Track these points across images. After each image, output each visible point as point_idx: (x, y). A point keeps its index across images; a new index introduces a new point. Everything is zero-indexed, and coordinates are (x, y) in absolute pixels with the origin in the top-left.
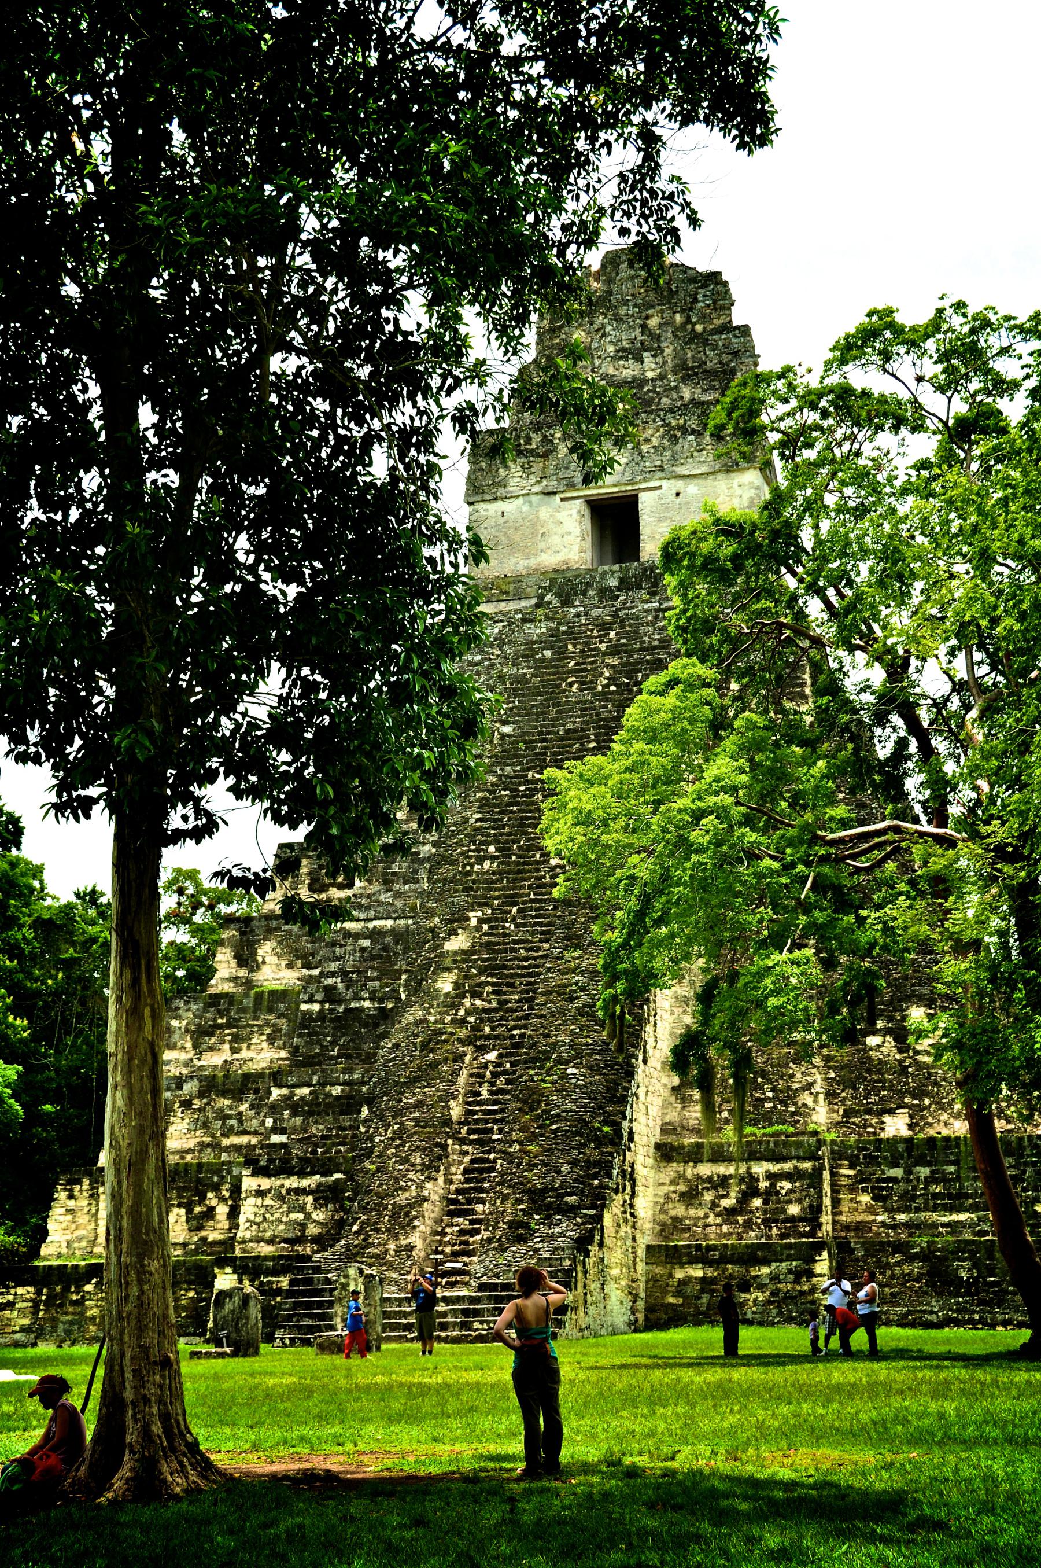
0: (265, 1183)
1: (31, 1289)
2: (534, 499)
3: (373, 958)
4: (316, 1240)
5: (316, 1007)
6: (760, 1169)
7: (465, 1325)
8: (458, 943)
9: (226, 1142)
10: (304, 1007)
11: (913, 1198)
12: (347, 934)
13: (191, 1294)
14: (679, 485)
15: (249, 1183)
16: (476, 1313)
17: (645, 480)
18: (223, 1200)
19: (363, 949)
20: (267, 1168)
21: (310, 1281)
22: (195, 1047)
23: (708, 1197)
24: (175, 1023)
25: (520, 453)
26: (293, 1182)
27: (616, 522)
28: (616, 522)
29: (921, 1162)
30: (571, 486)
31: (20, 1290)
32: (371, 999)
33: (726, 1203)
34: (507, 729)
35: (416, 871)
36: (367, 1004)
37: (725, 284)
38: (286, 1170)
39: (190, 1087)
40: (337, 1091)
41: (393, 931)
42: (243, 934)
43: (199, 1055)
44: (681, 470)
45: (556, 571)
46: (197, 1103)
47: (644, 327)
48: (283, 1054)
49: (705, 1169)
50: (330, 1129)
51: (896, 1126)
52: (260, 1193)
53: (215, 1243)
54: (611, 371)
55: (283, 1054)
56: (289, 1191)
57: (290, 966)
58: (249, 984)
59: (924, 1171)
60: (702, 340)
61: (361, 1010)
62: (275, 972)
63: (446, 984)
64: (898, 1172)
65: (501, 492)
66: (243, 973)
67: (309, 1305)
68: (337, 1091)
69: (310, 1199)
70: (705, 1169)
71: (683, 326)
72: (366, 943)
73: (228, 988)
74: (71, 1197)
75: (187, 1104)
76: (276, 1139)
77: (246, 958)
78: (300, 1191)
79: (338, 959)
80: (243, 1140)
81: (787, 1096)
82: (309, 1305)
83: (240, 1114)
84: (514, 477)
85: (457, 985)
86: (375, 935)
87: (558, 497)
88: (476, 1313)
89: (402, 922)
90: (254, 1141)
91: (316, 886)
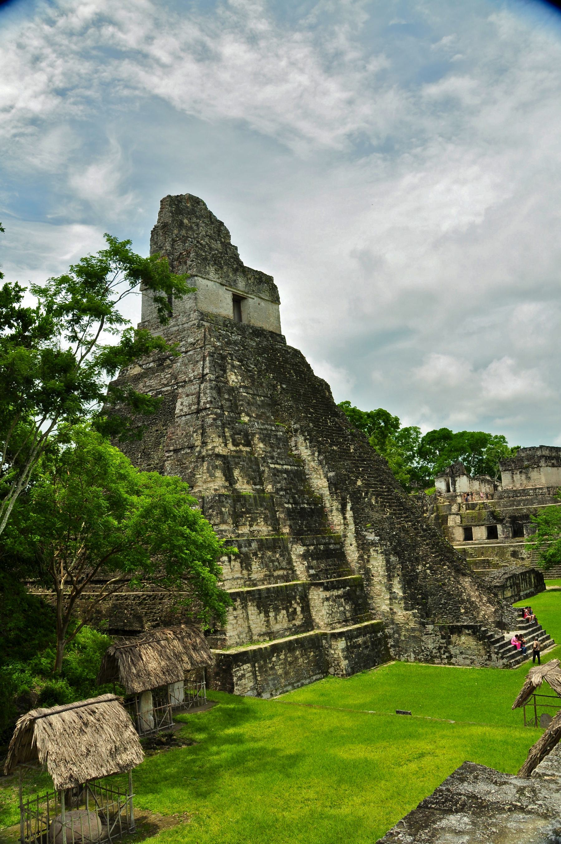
0: (328, 594)
1: (249, 665)
2: (217, 284)
5: (290, 506)
9: (276, 573)
10: (286, 505)
13: (312, 654)
14: (259, 300)
17: (251, 294)
19: (285, 479)
20: (327, 586)
26: (335, 593)
30: (230, 286)
31: (245, 667)
32: (307, 504)
35: (279, 444)
36: (306, 506)
39: (254, 545)
41: (292, 470)
42: (224, 463)
50: (326, 566)
56: (336, 596)
57: (248, 483)
61: (304, 508)
66: (227, 484)
69: (343, 600)
72: (285, 476)
74: (235, 609)
75: (255, 554)
78: (339, 597)
79: (279, 482)
80: (281, 573)
83: (277, 559)
86: (286, 471)
87: (225, 287)
89: (293, 467)
91: (235, 444)
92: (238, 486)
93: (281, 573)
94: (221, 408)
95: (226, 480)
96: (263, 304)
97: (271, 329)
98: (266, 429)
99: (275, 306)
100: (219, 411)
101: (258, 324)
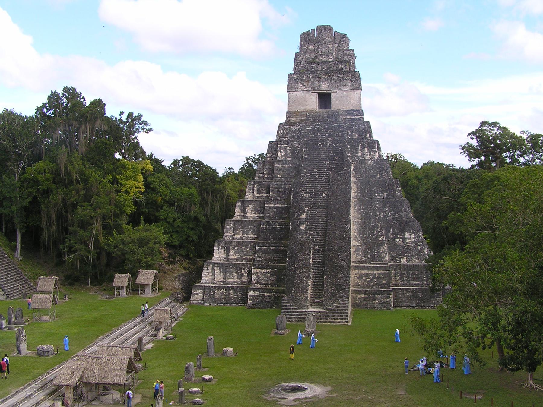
0: (258, 270)
3: (277, 214)
4: (271, 284)
5: (265, 226)
6: (376, 272)
7: (326, 319)
8: (304, 216)
9: (244, 257)
10: (262, 226)
11: (408, 278)
12: (270, 207)
14: (342, 91)
15: (254, 270)
16: (328, 316)
18: (246, 272)
19: (274, 212)
21: (286, 306)
22: (233, 232)
23: (364, 278)
24: (227, 227)
25: (301, 80)
27: (325, 99)
28: (325, 99)
29: (410, 270)
30: (314, 90)
33: (368, 280)
34: (306, 156)
37: (348, 38)
38: (263, 267)
39: (234, 244)
40: (273, 248)
41: (281, 207)
43: (234, 235)
44: (342, 88)
45: (310, 111)
46: (236, 248)
47: (328, 47)
48: (255, 236)
49: (363, 272)
51: (404, 261)
52: (257, 273)
53: (244, 282)
54: (321, 58)
55: (255, 236)
57: (255, 213)
58: (245, 217)
59: (411, 272)
60: (343, 51)
61: (276, 227)
62: (251, 214)
63: (302, 227)
64: (405, 272)
65: (297, 90)
66: (242, 214)
67: (287, 312)
68: (273, 248)
70: (363, 272)
71: (338, 47)
73: (239, 218)
75: (234, 248)
76: (258, 259)
77: (244, 211)
78: (267, 273)
80: (249, 257)
81: (380, 254)
82: (287, 312)
84: (300, 87)
85: (306, 228)
88: (328, 316)
90: (251, 257)
92: (248, 215)
93: (249, 257)
94: (263, 173)
95: (242, 212)
96: (345, 93)
97: (351, 108)
98: (277, 185)
99: (359, 91)
100: (262, 175)
101: (340, 108)
